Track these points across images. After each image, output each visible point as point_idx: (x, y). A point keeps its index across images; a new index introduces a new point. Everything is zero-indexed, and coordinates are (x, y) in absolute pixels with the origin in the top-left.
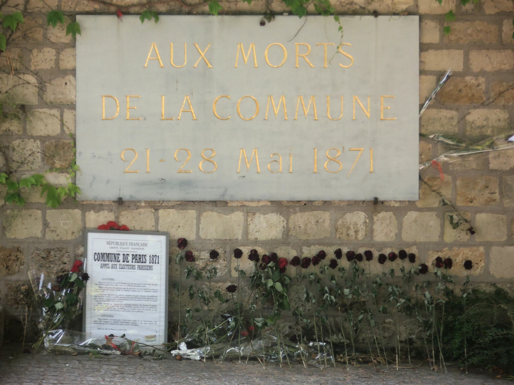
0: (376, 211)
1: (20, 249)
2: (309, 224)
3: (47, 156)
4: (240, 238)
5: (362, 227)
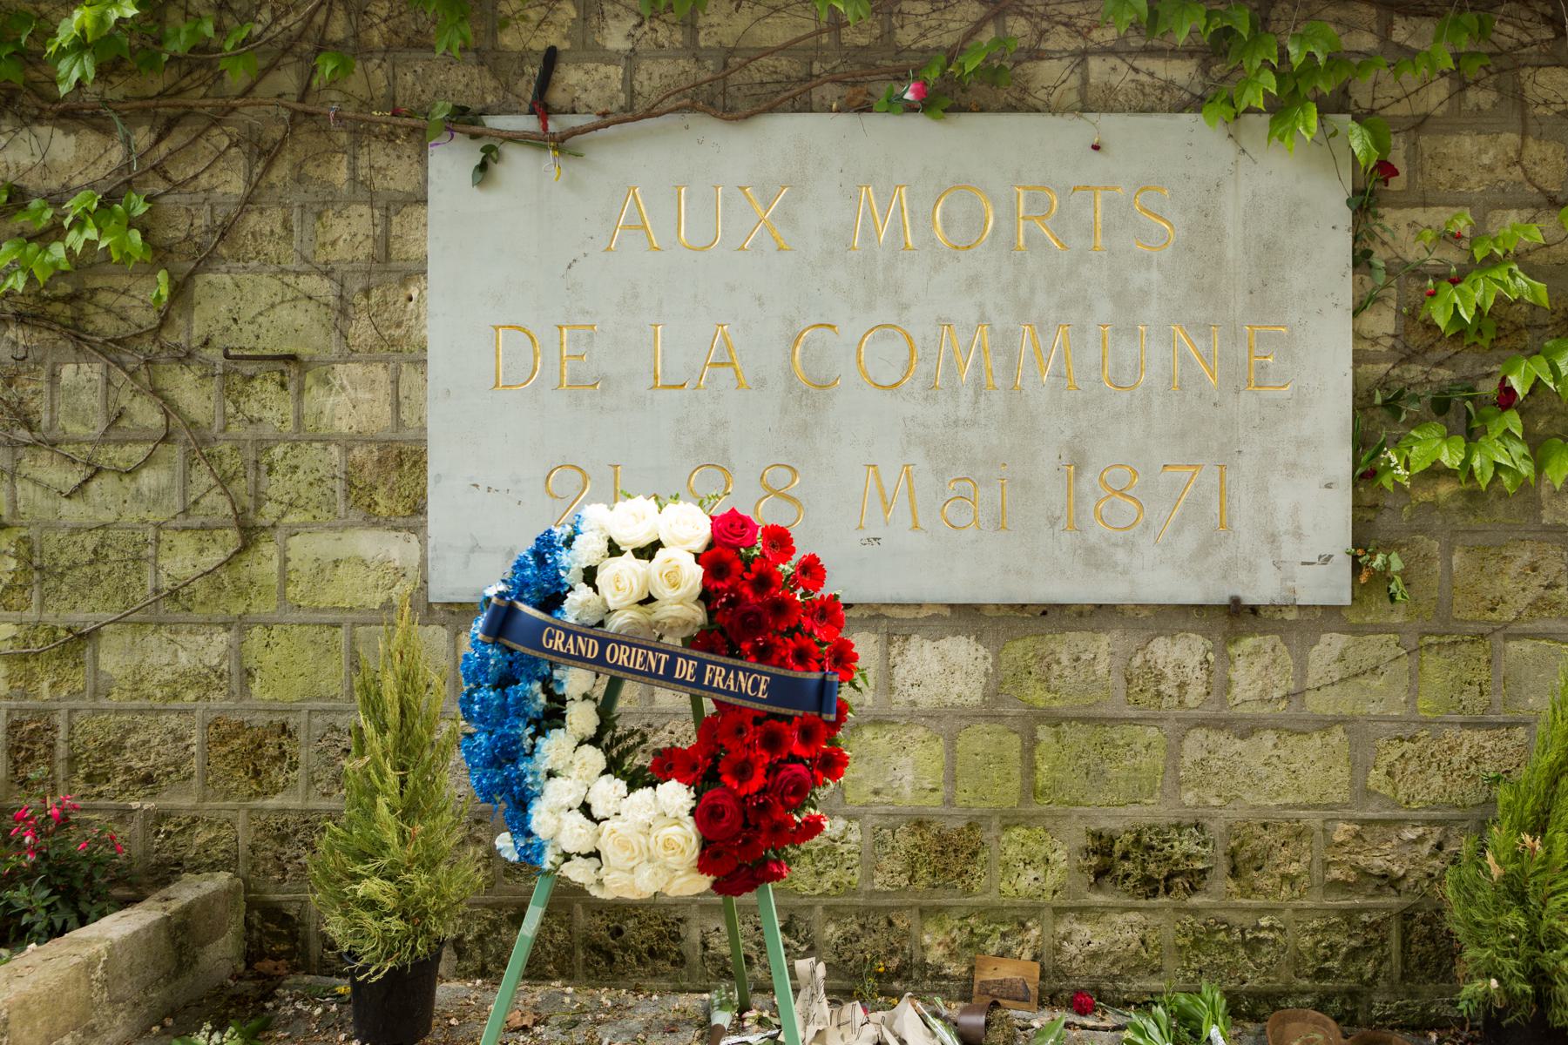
0: (1233, 637)
1: (290, 727)
2: (1055, 667)
3: (356, 487)
5: (1198, 673)
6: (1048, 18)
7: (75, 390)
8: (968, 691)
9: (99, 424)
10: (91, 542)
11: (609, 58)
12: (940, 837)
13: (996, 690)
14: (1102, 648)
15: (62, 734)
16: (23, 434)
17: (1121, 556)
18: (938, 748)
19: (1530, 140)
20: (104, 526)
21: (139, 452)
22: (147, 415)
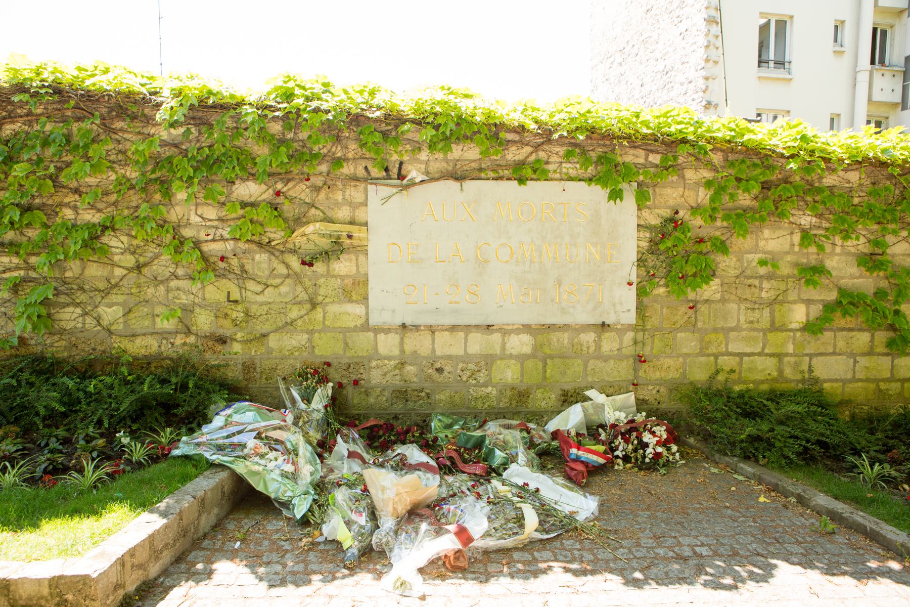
4: (498, 352)
6: (551, 152)
7: (260, 262)
8: (527, 350)
9: (267, 273)
10: (265, 308)
11: (421, 162)
12: (519, 392)
13: (535, 348)
14: (565, 337)
15: (258, 365)
16: (245, 276)
17: (571, 310)
18: (519, 366)
19: (686, 190)
20: (270, 303)
21: (278, 281)
22: (282, 270)
